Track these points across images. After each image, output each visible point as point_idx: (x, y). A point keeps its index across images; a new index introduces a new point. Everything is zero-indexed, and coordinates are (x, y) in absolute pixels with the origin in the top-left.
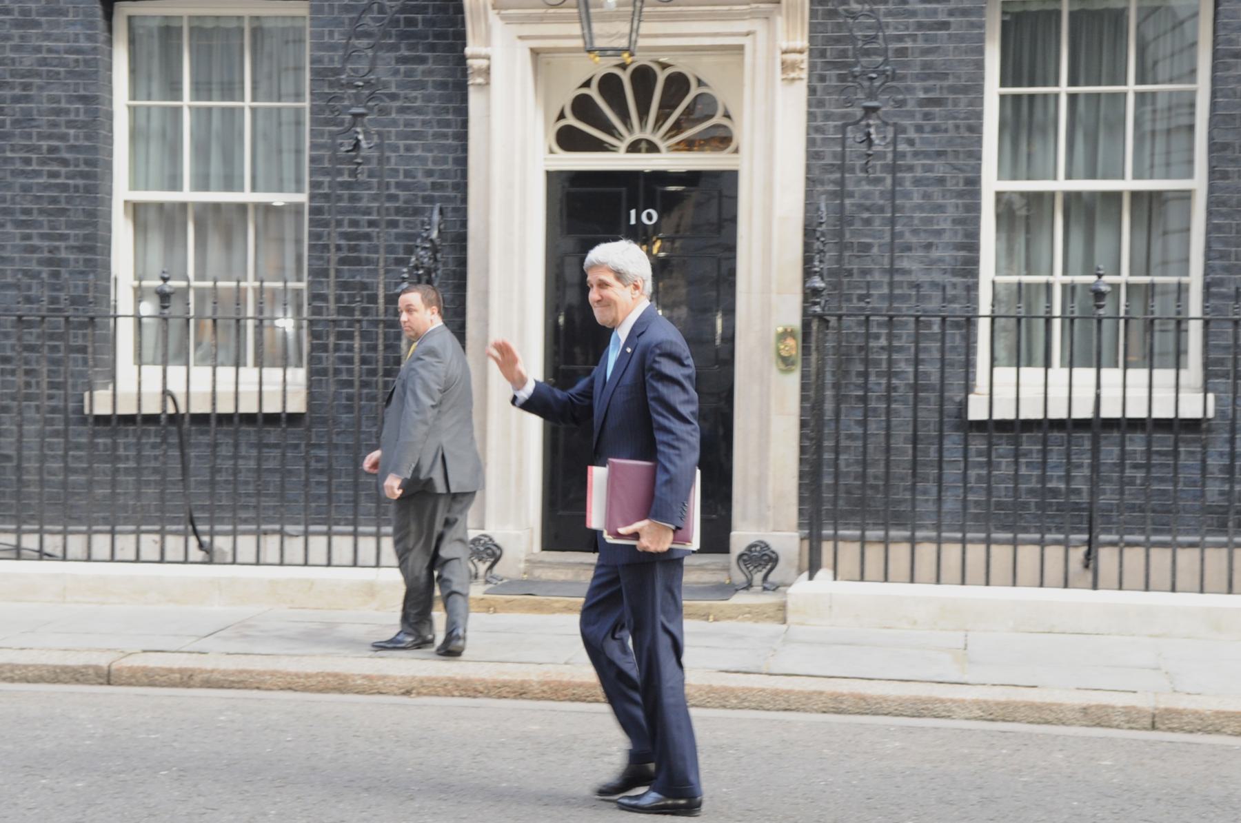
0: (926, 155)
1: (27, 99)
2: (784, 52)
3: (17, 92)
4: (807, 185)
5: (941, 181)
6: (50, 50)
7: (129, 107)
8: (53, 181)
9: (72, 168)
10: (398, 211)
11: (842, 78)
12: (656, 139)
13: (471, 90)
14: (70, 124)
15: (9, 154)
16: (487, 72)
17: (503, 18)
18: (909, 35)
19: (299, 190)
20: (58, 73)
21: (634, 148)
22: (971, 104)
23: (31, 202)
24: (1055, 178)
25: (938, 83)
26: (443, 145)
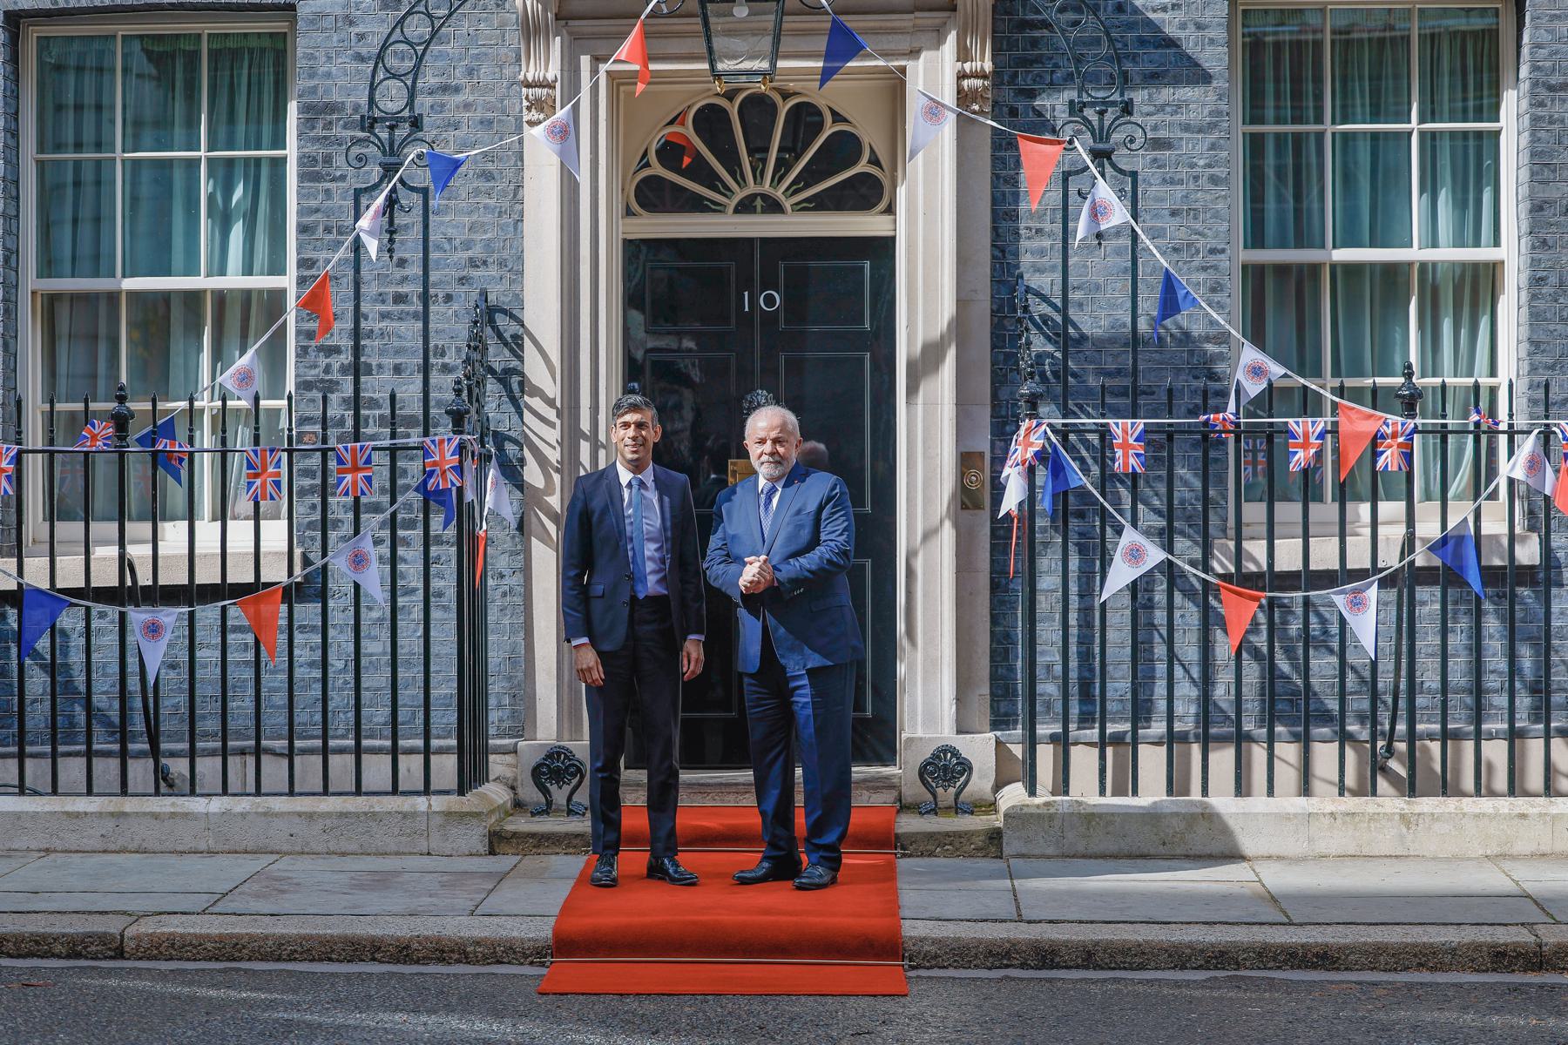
4: (993, 257)
5: (1175, 250)
7: (41, 165)
12: (779, 193)
17: (570, 33)
18: (1127, 56)
19: (277, 268)
21: (745, 207)
22: (1213, 147)
24: (1323, 246)
25: (1168, 118)
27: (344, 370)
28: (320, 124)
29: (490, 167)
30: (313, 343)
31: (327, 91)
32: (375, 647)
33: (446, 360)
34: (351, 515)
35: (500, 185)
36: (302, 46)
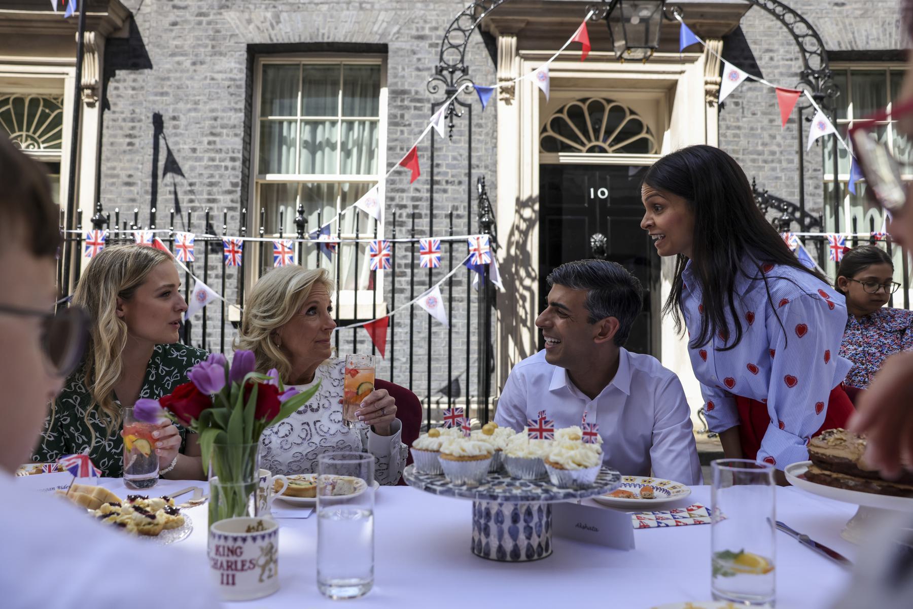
0: (790, 154)
1: (195, 110)
2: (706, 83)
3: (189, 106)
6: (213, 79)
8: (211, 163)
9: (223, 155)
10: (447, 182)
11: (737, 104)
12: (605, 146)
13: (501, 105)
14: (223, 127)
15: (181, 146)
16: (510, 91)
18: (775, 80)
20: (217, 93)
21: (591, 150)
23: (195, 177)
26: (479, 140)
27: (408, 216)
28: (399, 100)
29: (480, 121)
30: (394, 203)
31: (403, 84)
32: (421, 351)
33: (459, 212)
34: (409, 287)
35: (484, 131)
36: (391, 62)
